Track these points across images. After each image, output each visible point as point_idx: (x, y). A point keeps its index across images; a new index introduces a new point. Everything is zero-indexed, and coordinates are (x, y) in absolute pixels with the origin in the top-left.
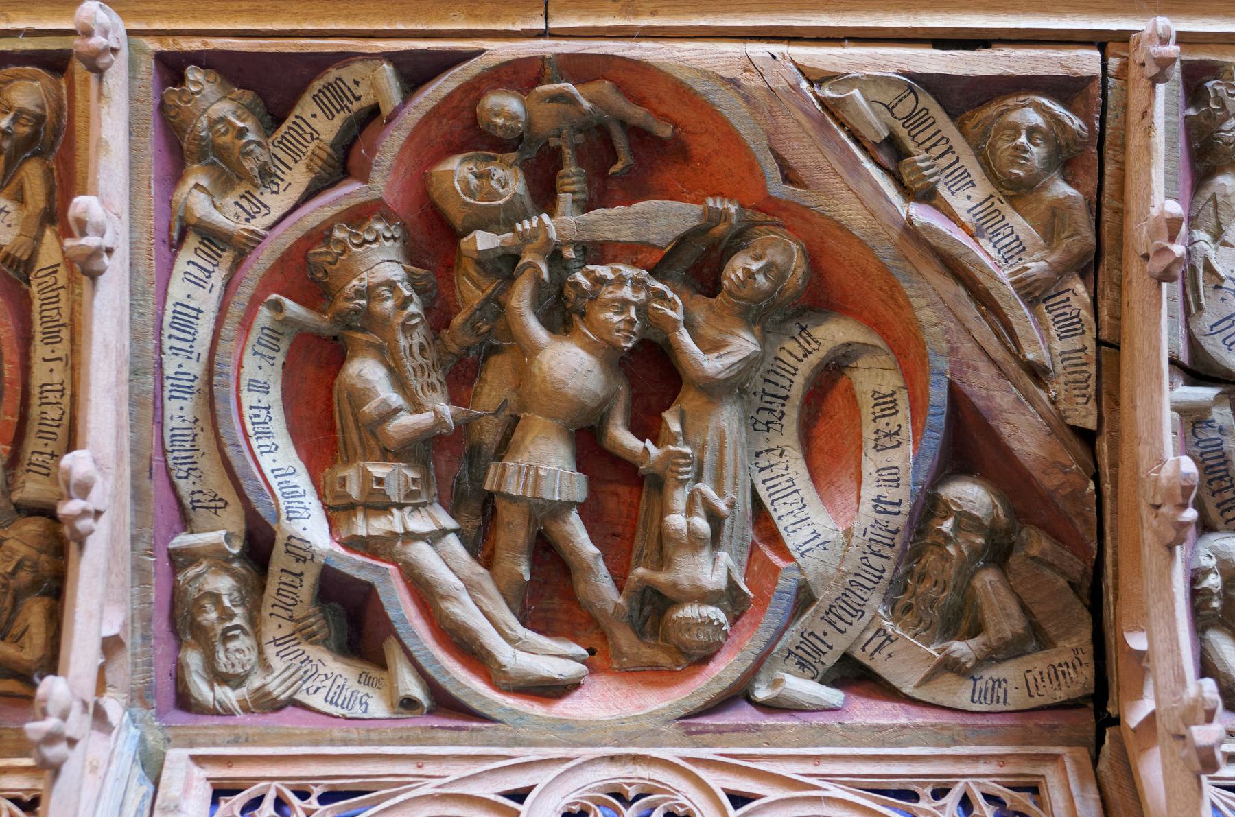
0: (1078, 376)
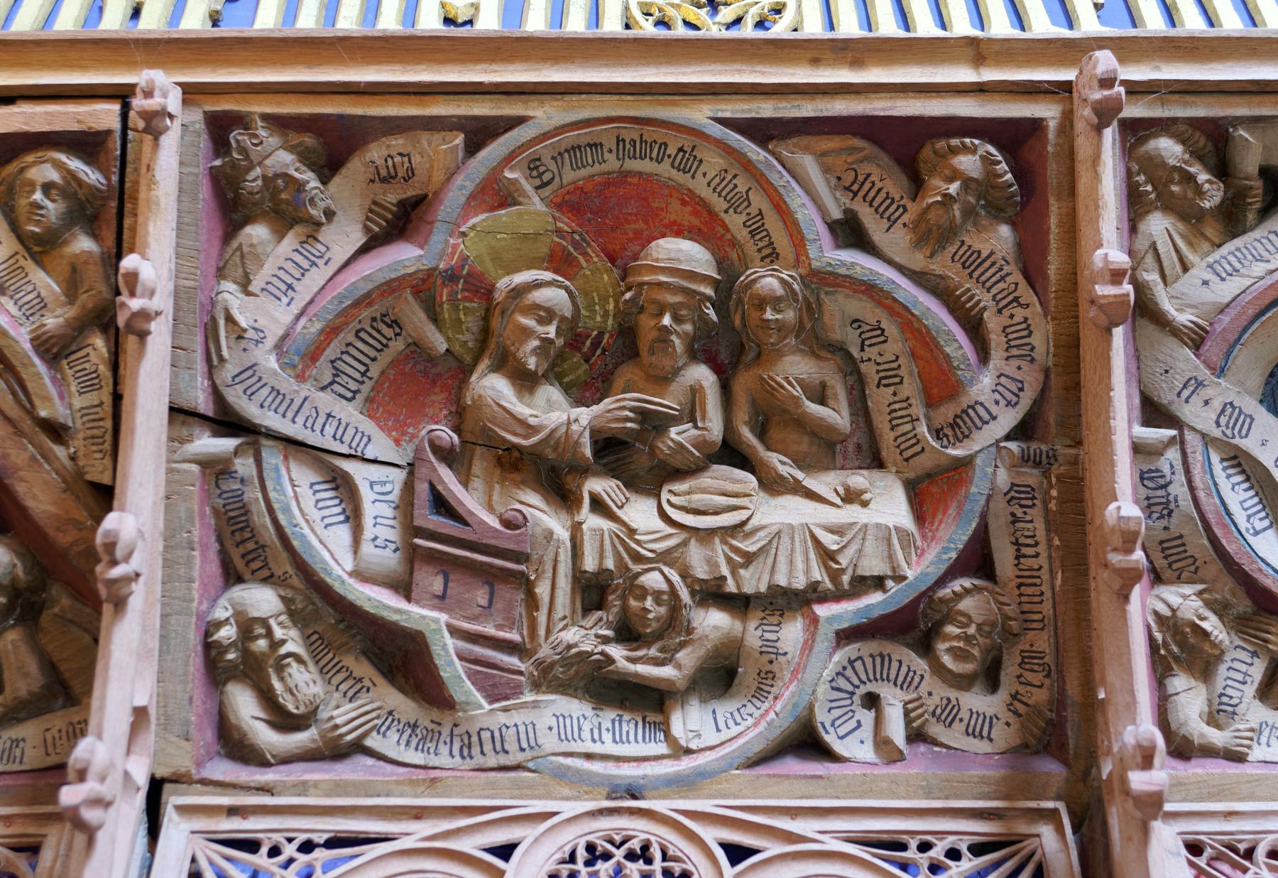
0: (95, 432)
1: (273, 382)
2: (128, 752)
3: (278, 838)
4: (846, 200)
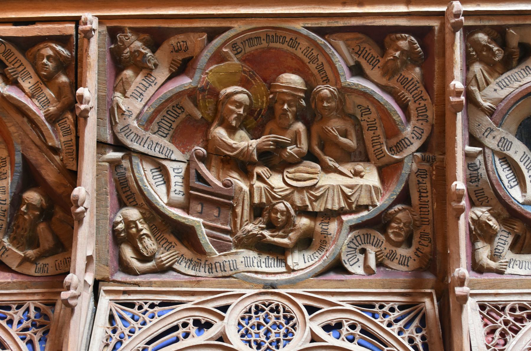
0: (70, 151)
1: (135, 131)
2: (86, 272)
3: (141, 302)
4: (356, 58)
